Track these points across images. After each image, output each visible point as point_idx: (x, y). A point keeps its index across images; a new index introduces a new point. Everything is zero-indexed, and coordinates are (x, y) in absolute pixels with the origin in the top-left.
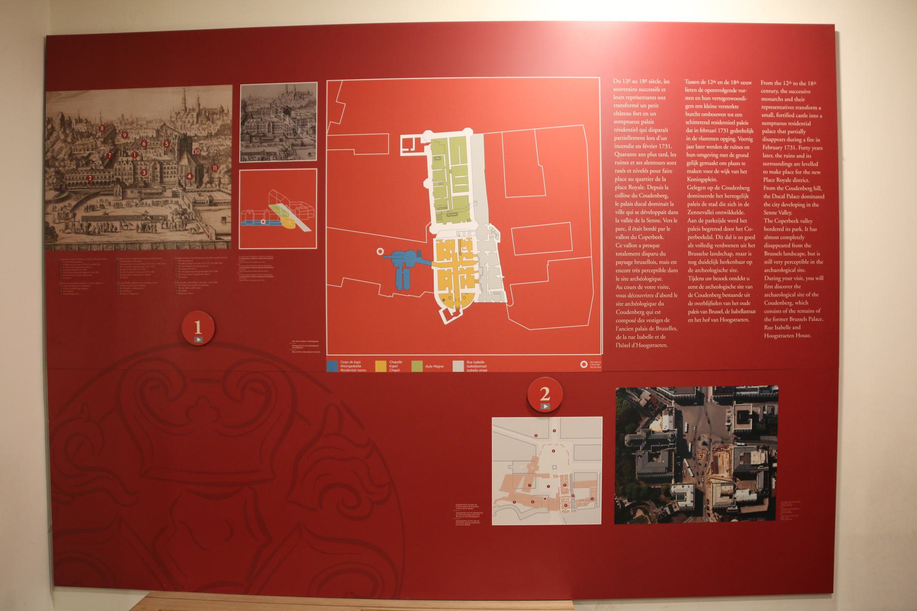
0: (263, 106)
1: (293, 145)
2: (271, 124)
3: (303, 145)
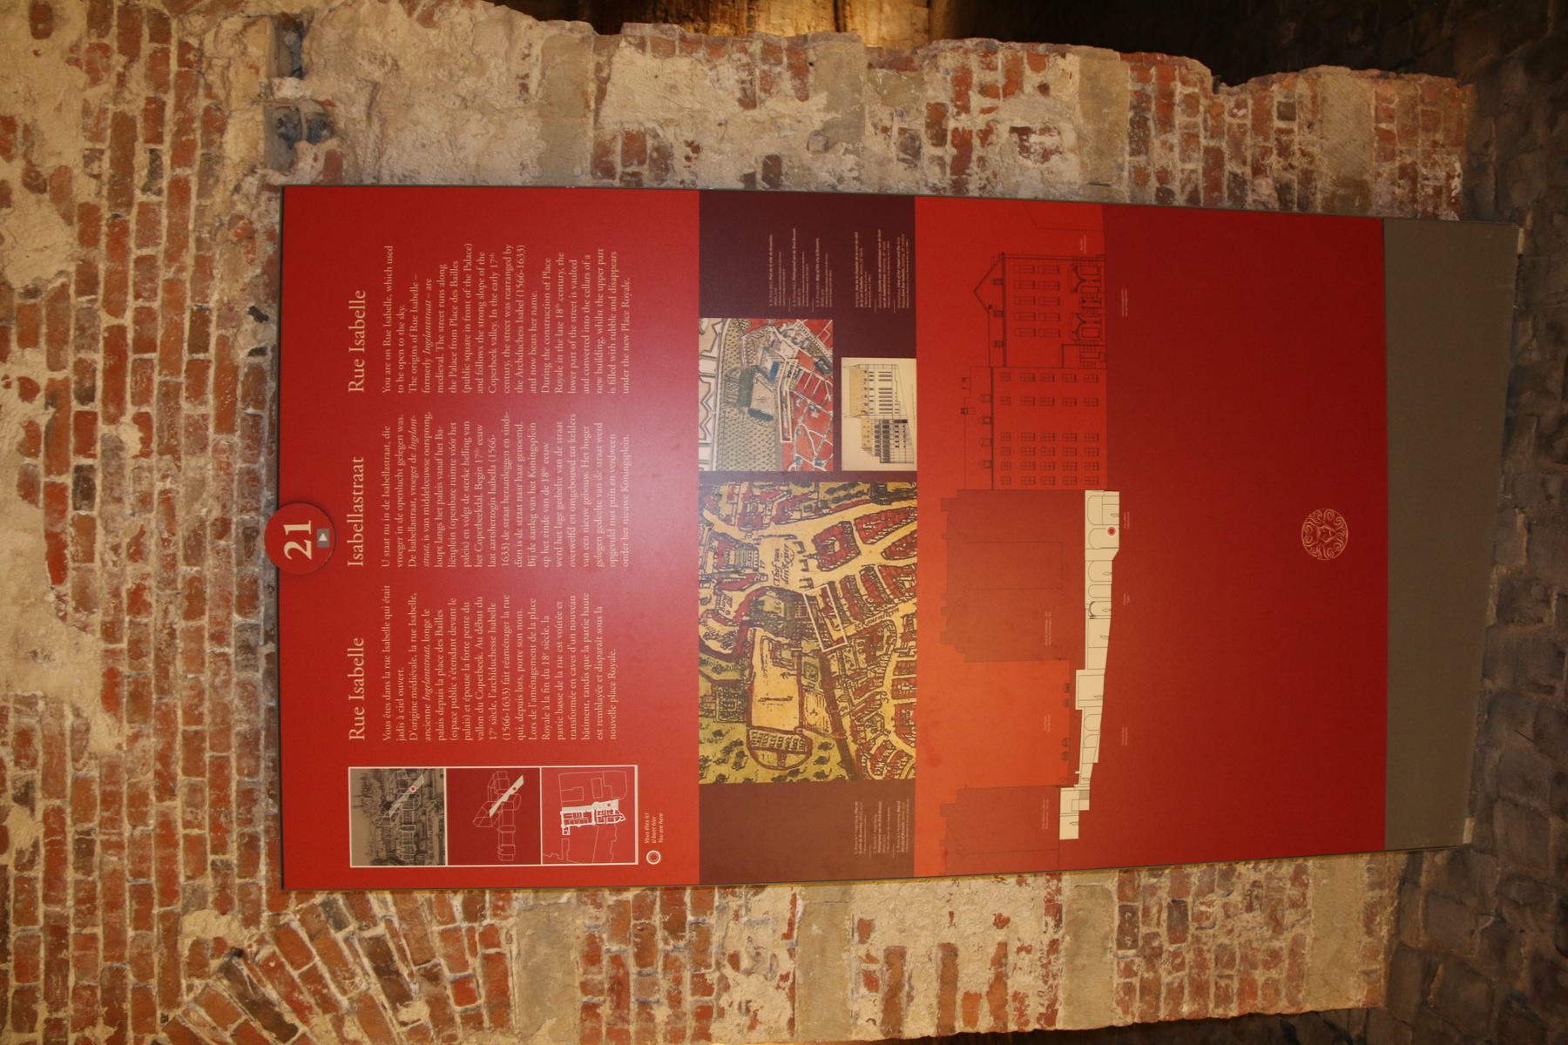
1: (430, 798)
3: (430, 785)
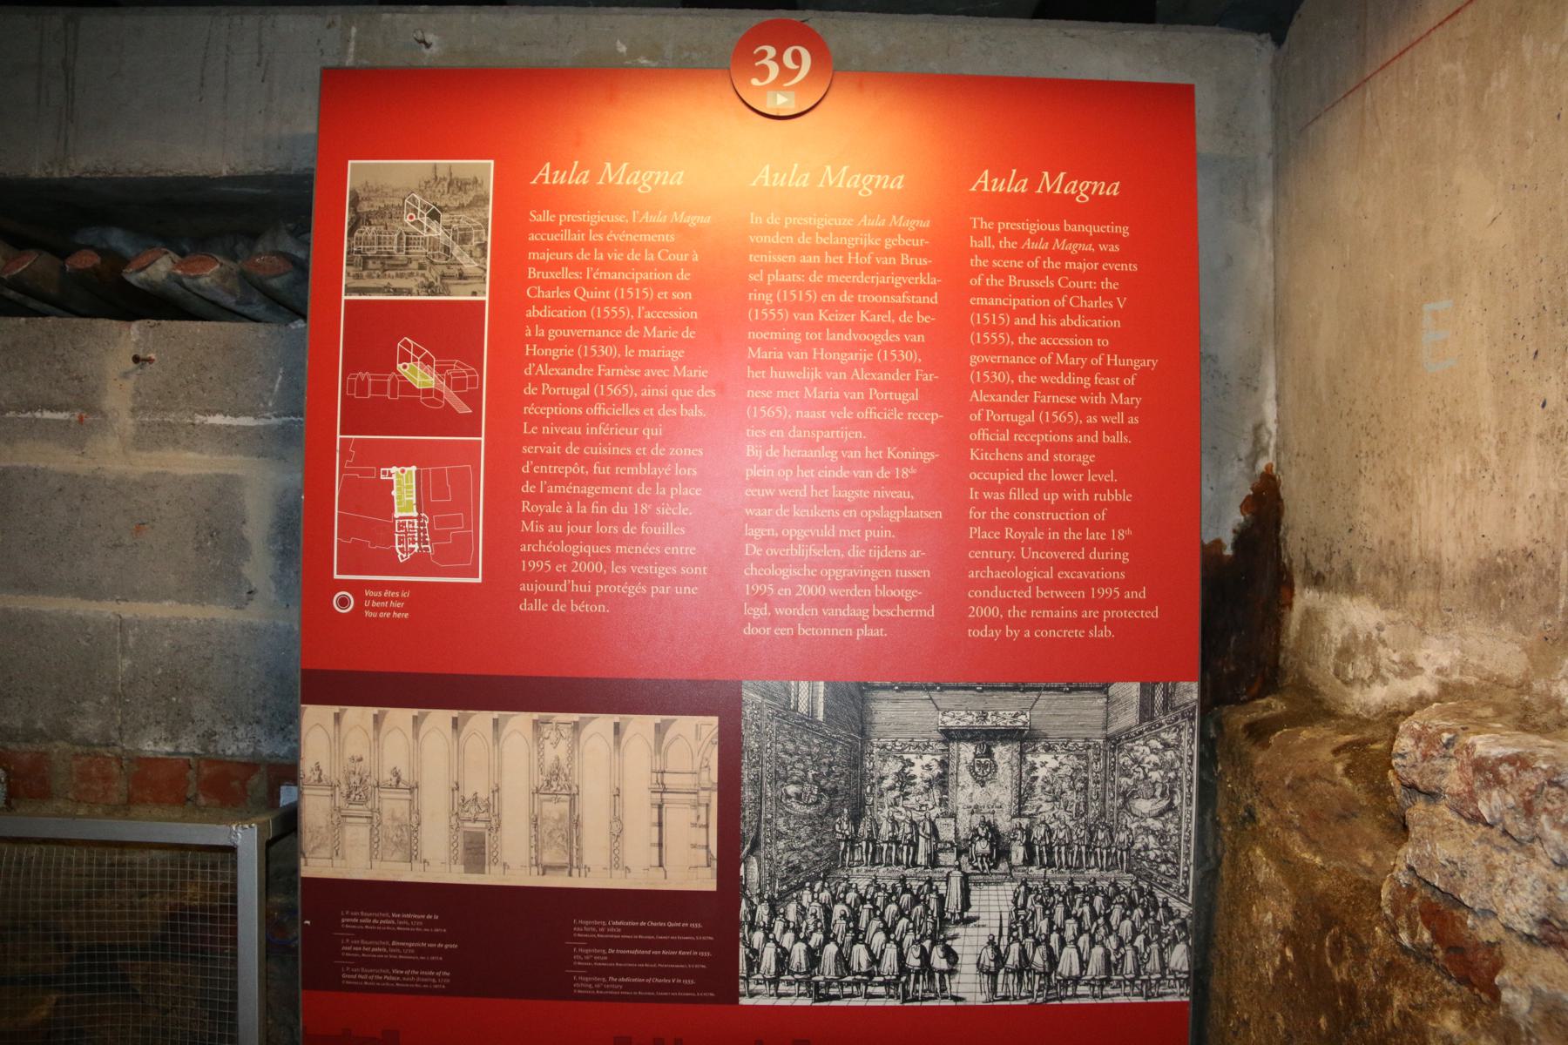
0: (390, 203)
1: (443, 276)
2: (405, 236)
3: (462, 276)
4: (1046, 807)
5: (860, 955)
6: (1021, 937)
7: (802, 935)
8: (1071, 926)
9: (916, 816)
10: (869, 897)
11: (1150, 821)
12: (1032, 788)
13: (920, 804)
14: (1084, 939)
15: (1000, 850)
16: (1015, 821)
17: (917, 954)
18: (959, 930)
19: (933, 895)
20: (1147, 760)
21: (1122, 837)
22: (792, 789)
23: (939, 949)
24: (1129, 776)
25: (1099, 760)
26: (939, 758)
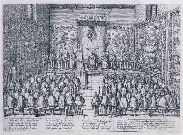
4: (114, 49)
5: (51, 100)
6: (106, 94)
7: (31, 94)
8: (124, 90)
9: (69, 52)
10: (53, 80)
11: (151, 54)
12: (109, 42)
13: (69, 48)
14: (128, 95)
15: (98, 63)
16: (104, 53)
17: (71, 99)
18: (85, 91)
19: (76, 79)
20: (149, 33)
21: (141, 59)
22: (26, 43)
23: (78, 98)
24: (143, 38)
25: (132, 32)
26: (76, 32)
